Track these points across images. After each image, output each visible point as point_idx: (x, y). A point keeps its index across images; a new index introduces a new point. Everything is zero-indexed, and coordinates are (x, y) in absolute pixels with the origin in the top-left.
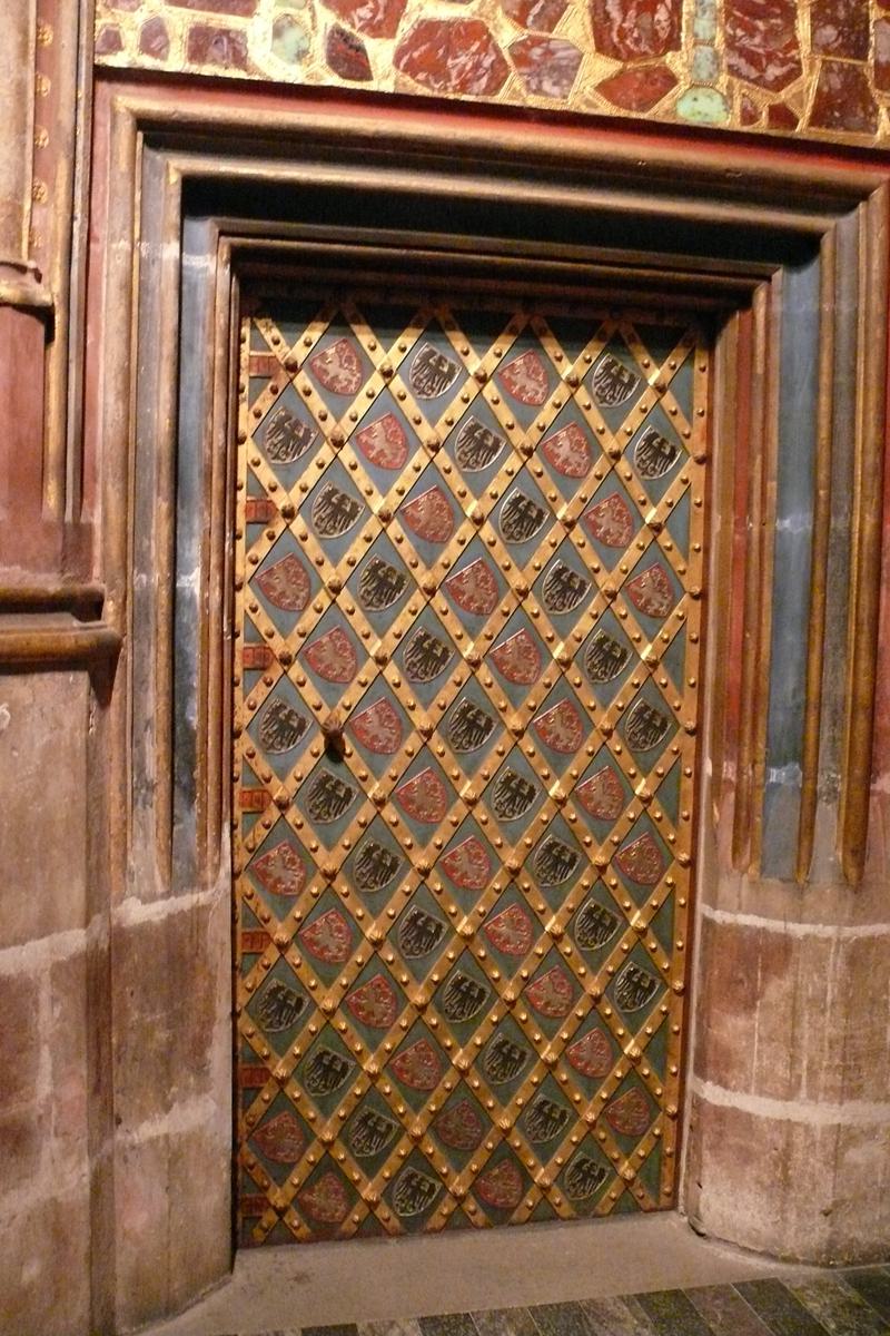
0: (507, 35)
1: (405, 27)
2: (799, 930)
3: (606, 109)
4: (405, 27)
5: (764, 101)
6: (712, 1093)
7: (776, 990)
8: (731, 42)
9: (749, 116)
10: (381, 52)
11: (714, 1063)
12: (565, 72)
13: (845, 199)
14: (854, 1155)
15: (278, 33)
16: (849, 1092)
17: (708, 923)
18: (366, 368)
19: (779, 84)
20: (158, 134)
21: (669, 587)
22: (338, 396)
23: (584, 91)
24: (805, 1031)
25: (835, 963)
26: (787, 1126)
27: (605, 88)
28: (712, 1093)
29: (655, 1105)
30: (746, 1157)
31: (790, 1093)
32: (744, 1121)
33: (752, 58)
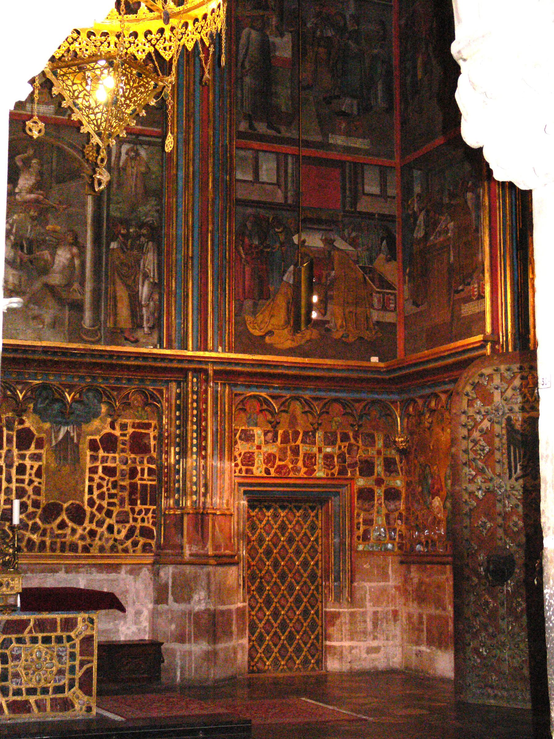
0: (291, 466)
1: (275, 466)
2: (341, 610)
3: (305, 476)
4: (275, 466)
5: (330, 473)
6: (328, 643)
7: (338, 622)
8: (324, 463)
9: (327, 475)
10: (272, 470)
11: (328, 637)
12: (299, 471)
13: (342, 486)
14: (353, 651)
15: (257, 469)
16: (352, 639)
17: (325, 612)
18: (265, 516)
19: (332, 469)
20: (240, 484)
21: (316, 551)
22: (261, 521)
23: (302, 474)
24: (343, 628)
25: (347, 615)
26: (341, 647)
27: (305, 473)
28: (328, 643)
29: (317, 650)
30: (335, 654)
31: (342, 640)
32: (334, 647)
33: (327, 465)
